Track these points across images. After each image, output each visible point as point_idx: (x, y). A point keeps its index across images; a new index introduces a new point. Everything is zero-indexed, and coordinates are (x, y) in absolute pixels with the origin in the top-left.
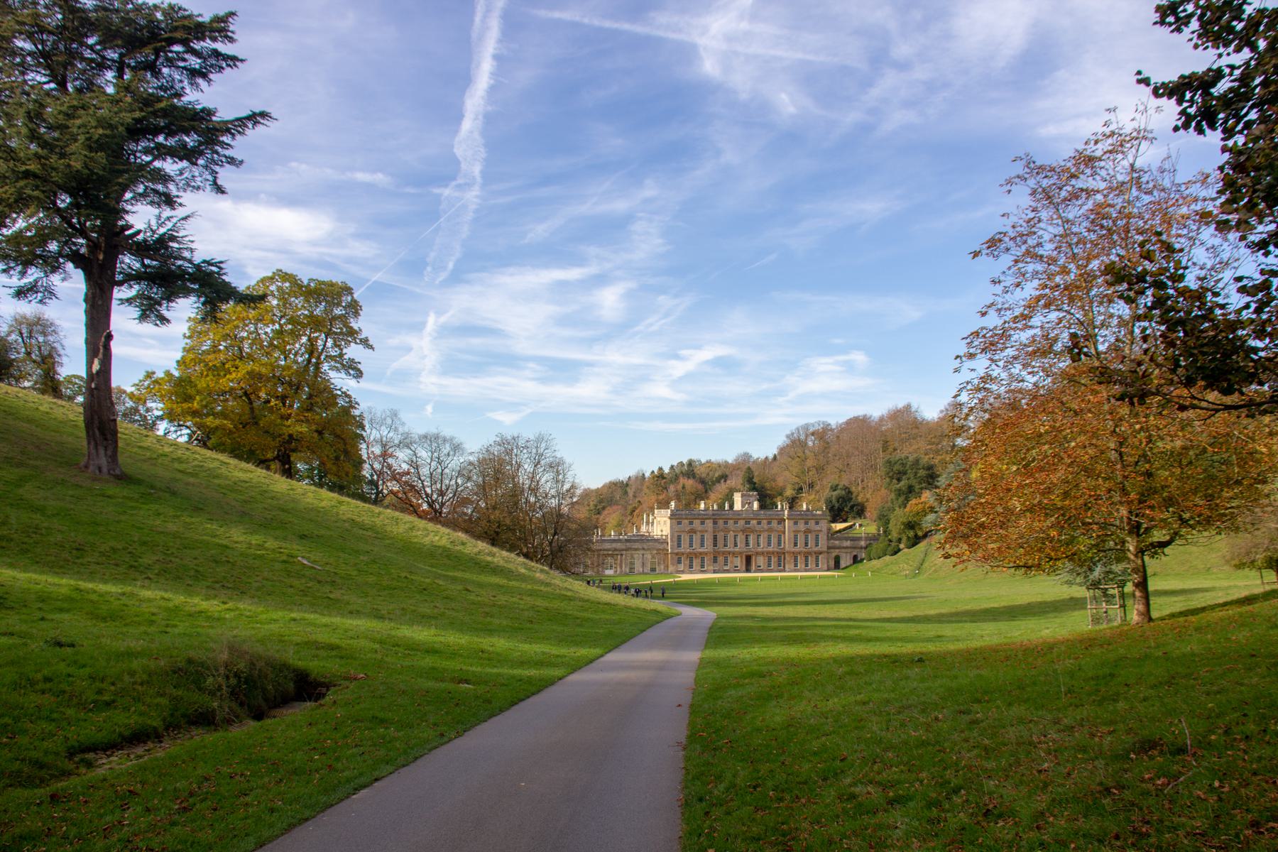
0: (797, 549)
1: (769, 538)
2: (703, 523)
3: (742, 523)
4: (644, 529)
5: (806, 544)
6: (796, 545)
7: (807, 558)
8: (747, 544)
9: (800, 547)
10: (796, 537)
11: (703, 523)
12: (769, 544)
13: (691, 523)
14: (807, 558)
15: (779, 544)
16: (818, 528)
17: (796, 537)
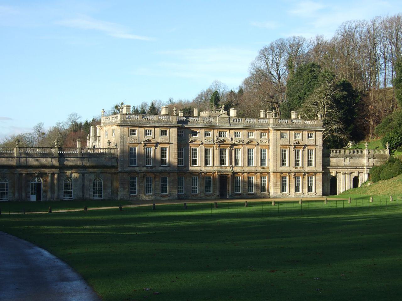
0: (285, 168)
1: (249, 152)
2: (163, 133)
3: (214, 134)
4: (90, 144)
5: (296, 163)
6: (283, 163)
7: (296, 178)
8: (222, 162)
9: (289, 165)
10: (283, 152)
11: (163, 133)
12: (249, 163)
13: (148, 133)
14: (296, 178)
15: (262, 163)
16: (310, 142)
17: (283, 152)
